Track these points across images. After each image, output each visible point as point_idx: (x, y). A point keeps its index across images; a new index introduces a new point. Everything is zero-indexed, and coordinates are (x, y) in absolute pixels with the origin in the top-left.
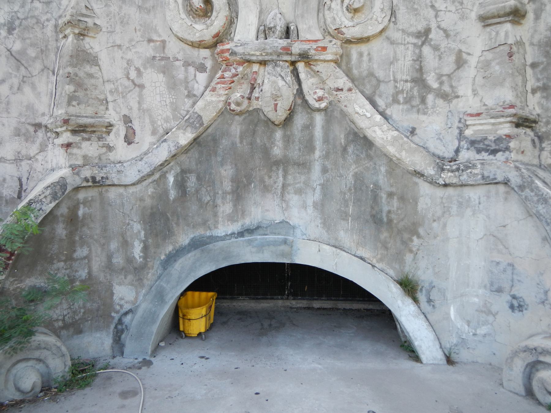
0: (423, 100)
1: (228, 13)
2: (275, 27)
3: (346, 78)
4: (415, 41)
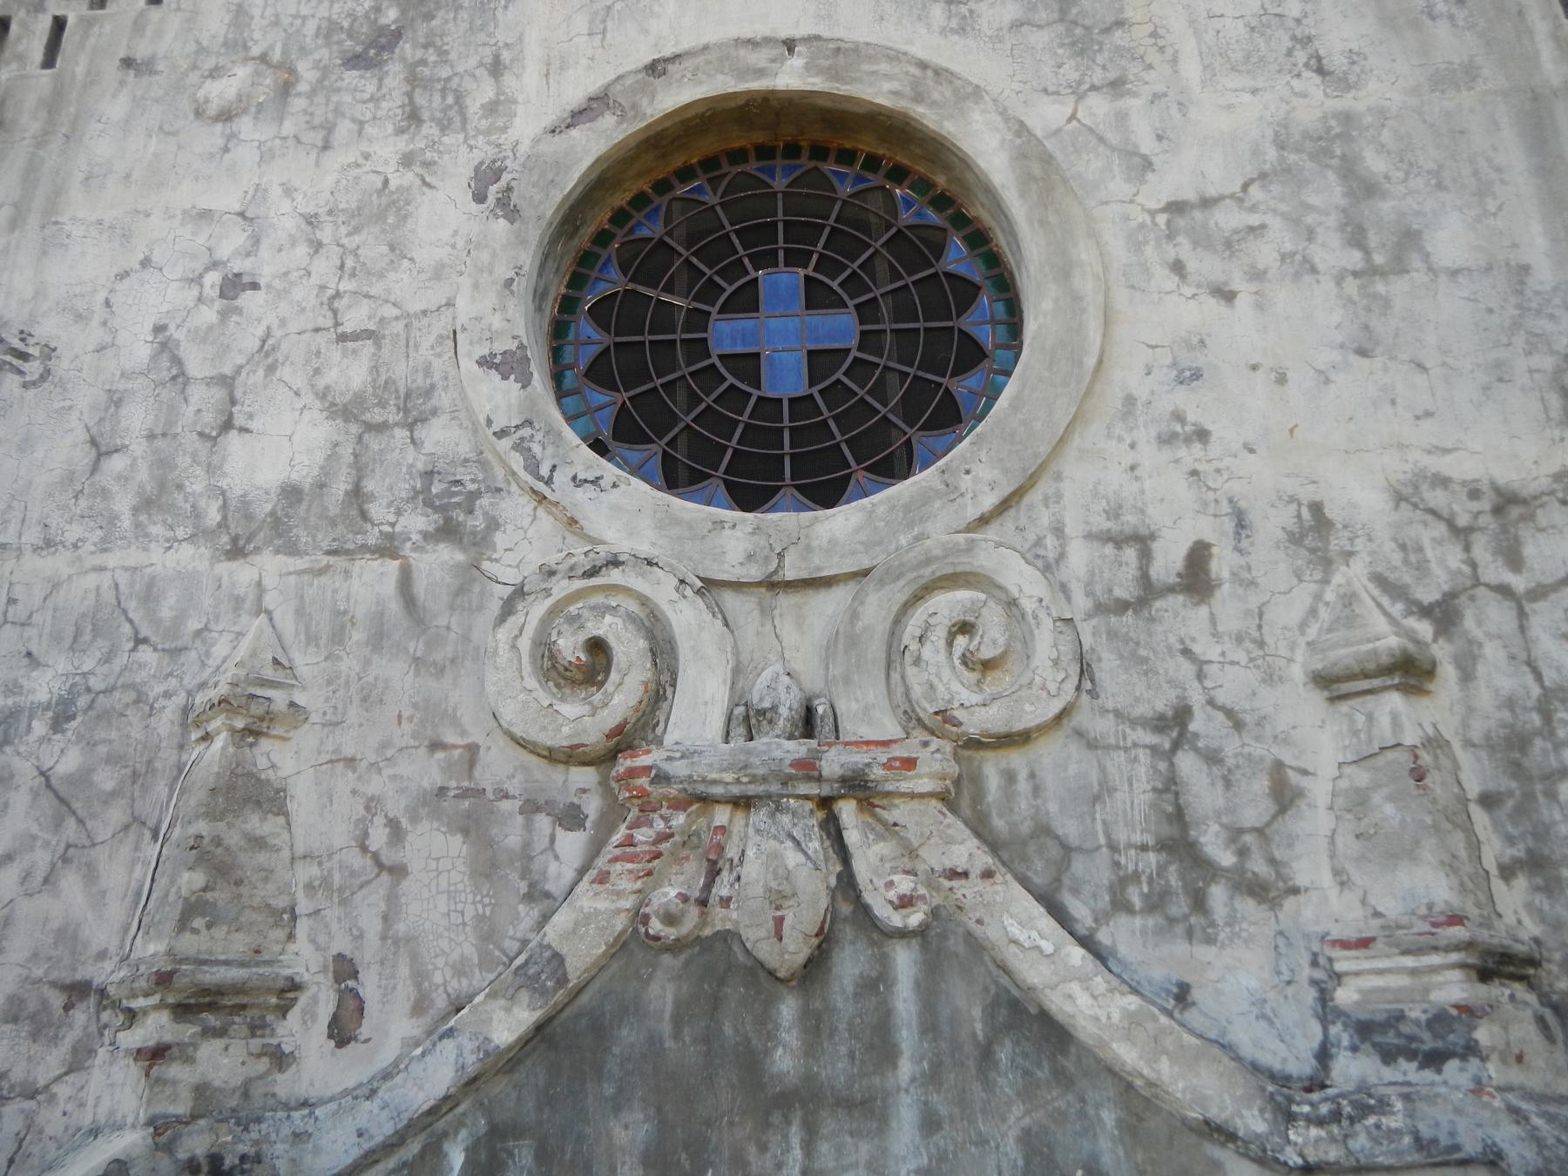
0: (1199, 902)
1: (649, 675)
2: (774, 708)
3: (973, 842)
4: (1152, 739)
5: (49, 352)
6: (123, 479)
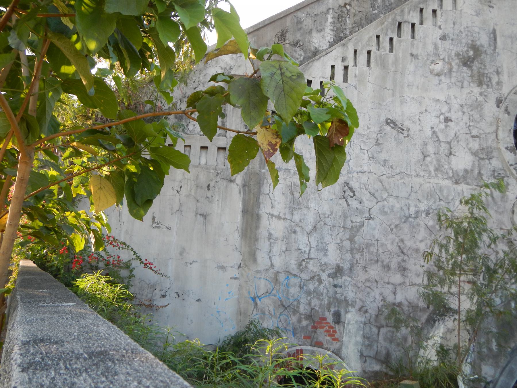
5: (408, 130)
6: (431, 163)
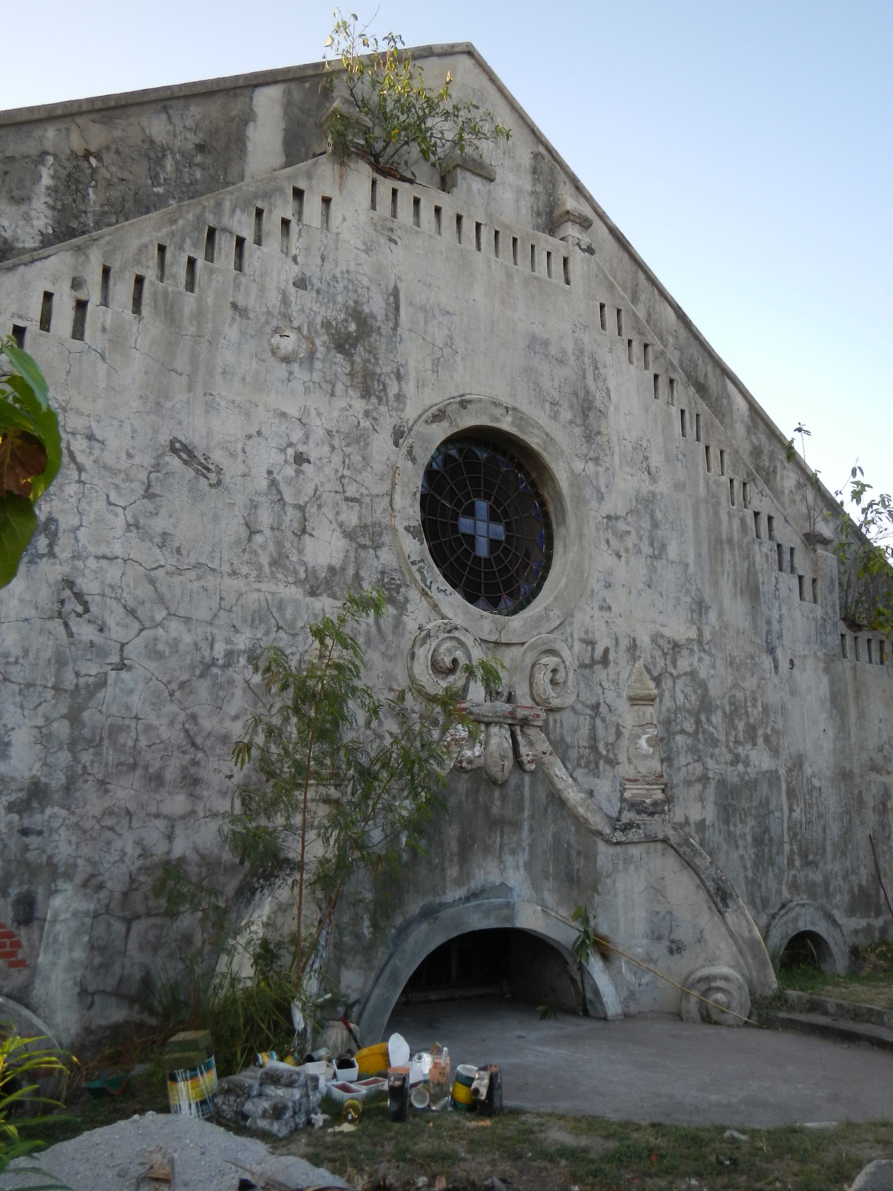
0: (597, 767)
4: (590, 712)
5: (219, 471)
6: (263, 547)
